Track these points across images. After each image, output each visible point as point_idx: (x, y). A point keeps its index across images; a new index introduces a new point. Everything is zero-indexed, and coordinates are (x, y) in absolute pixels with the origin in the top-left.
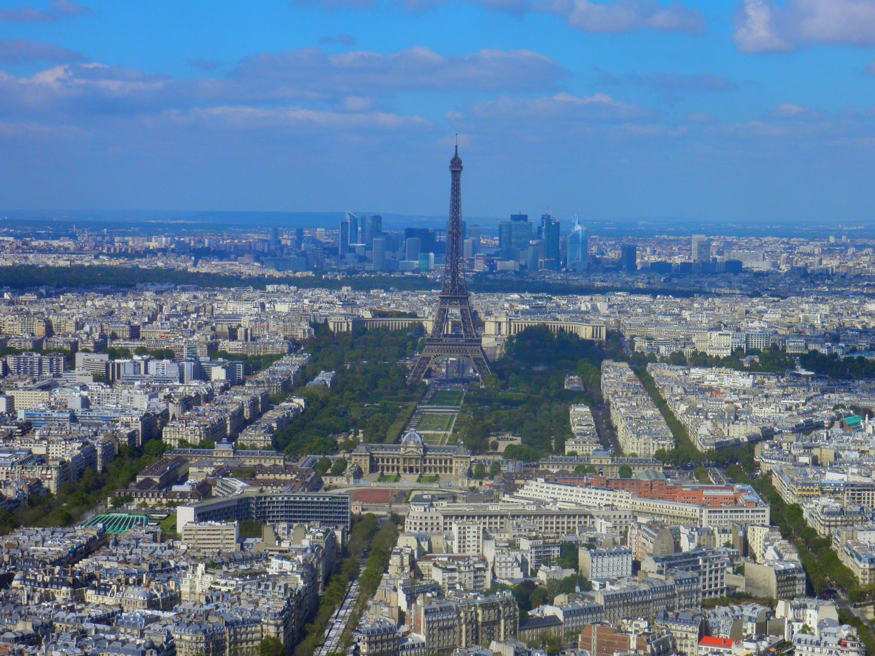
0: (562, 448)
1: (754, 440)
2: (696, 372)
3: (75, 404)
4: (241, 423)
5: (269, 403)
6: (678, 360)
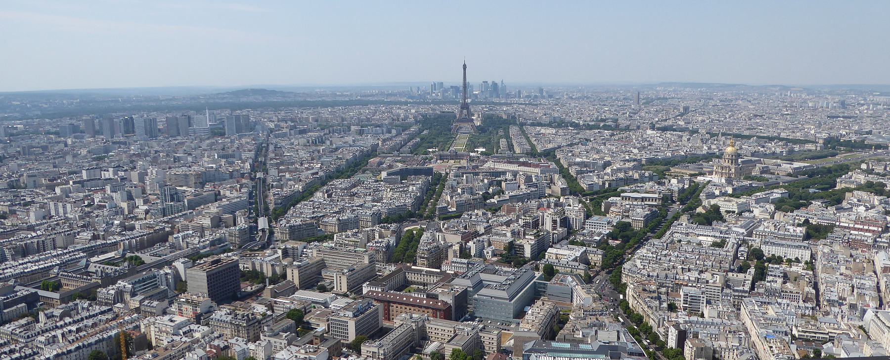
0: (497, 151)
1: (554, 149)
2: (538, 128)
6: (533, 125)
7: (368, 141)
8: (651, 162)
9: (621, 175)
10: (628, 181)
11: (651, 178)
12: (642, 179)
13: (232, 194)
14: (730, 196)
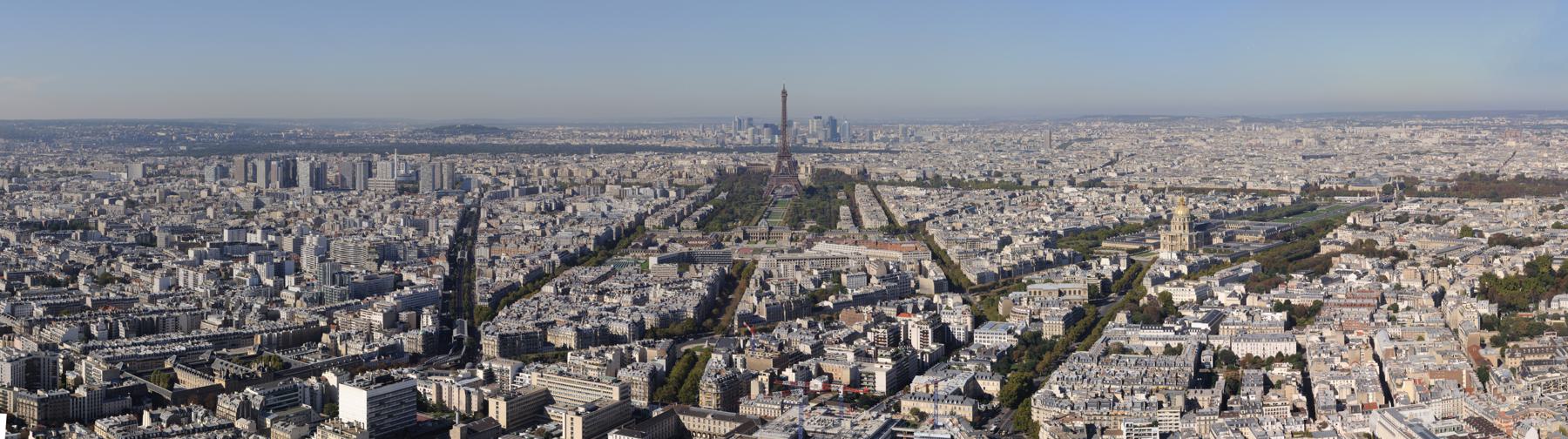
1: (926, 220)
3: (604, 209)
4: (682, 217)
5: (696, 207)
7: (628, 210)
8: (1073, 233)
9: (1027, 257)
10: (1041, 265)
11: (1070, 261)
12: (1060, 261)
13: (422, 280)
14: (1188, 278)
